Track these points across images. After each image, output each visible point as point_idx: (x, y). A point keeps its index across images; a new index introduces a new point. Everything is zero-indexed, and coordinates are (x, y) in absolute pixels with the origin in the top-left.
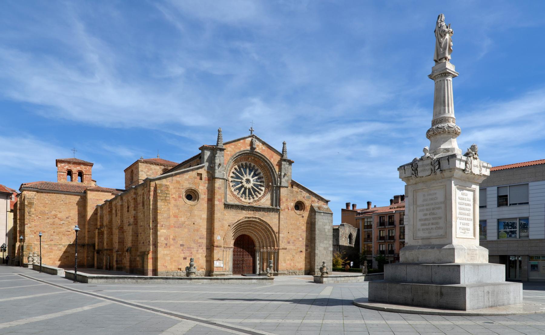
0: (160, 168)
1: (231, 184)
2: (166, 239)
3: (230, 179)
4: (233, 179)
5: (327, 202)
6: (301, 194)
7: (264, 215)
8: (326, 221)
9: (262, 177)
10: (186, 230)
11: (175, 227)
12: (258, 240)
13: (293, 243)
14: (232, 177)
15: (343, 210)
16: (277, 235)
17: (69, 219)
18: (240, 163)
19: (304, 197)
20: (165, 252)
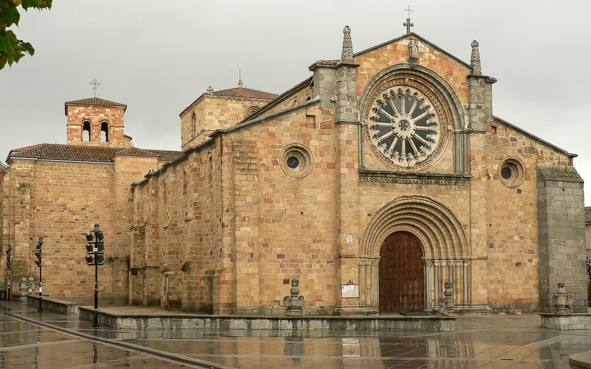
0: (244, 106)
1: (373, 133)
2: (251, 245)
3: (371, 123)
4: (375, 123)
6: (514, 145)
7: (439, 192)
11: (267, 221)
13: (501, 246)
14: (373, 118)
16: (467, 231)
17: (87, 212)
18: (388, 91)
19: (520, 151)
20: (250, 270)
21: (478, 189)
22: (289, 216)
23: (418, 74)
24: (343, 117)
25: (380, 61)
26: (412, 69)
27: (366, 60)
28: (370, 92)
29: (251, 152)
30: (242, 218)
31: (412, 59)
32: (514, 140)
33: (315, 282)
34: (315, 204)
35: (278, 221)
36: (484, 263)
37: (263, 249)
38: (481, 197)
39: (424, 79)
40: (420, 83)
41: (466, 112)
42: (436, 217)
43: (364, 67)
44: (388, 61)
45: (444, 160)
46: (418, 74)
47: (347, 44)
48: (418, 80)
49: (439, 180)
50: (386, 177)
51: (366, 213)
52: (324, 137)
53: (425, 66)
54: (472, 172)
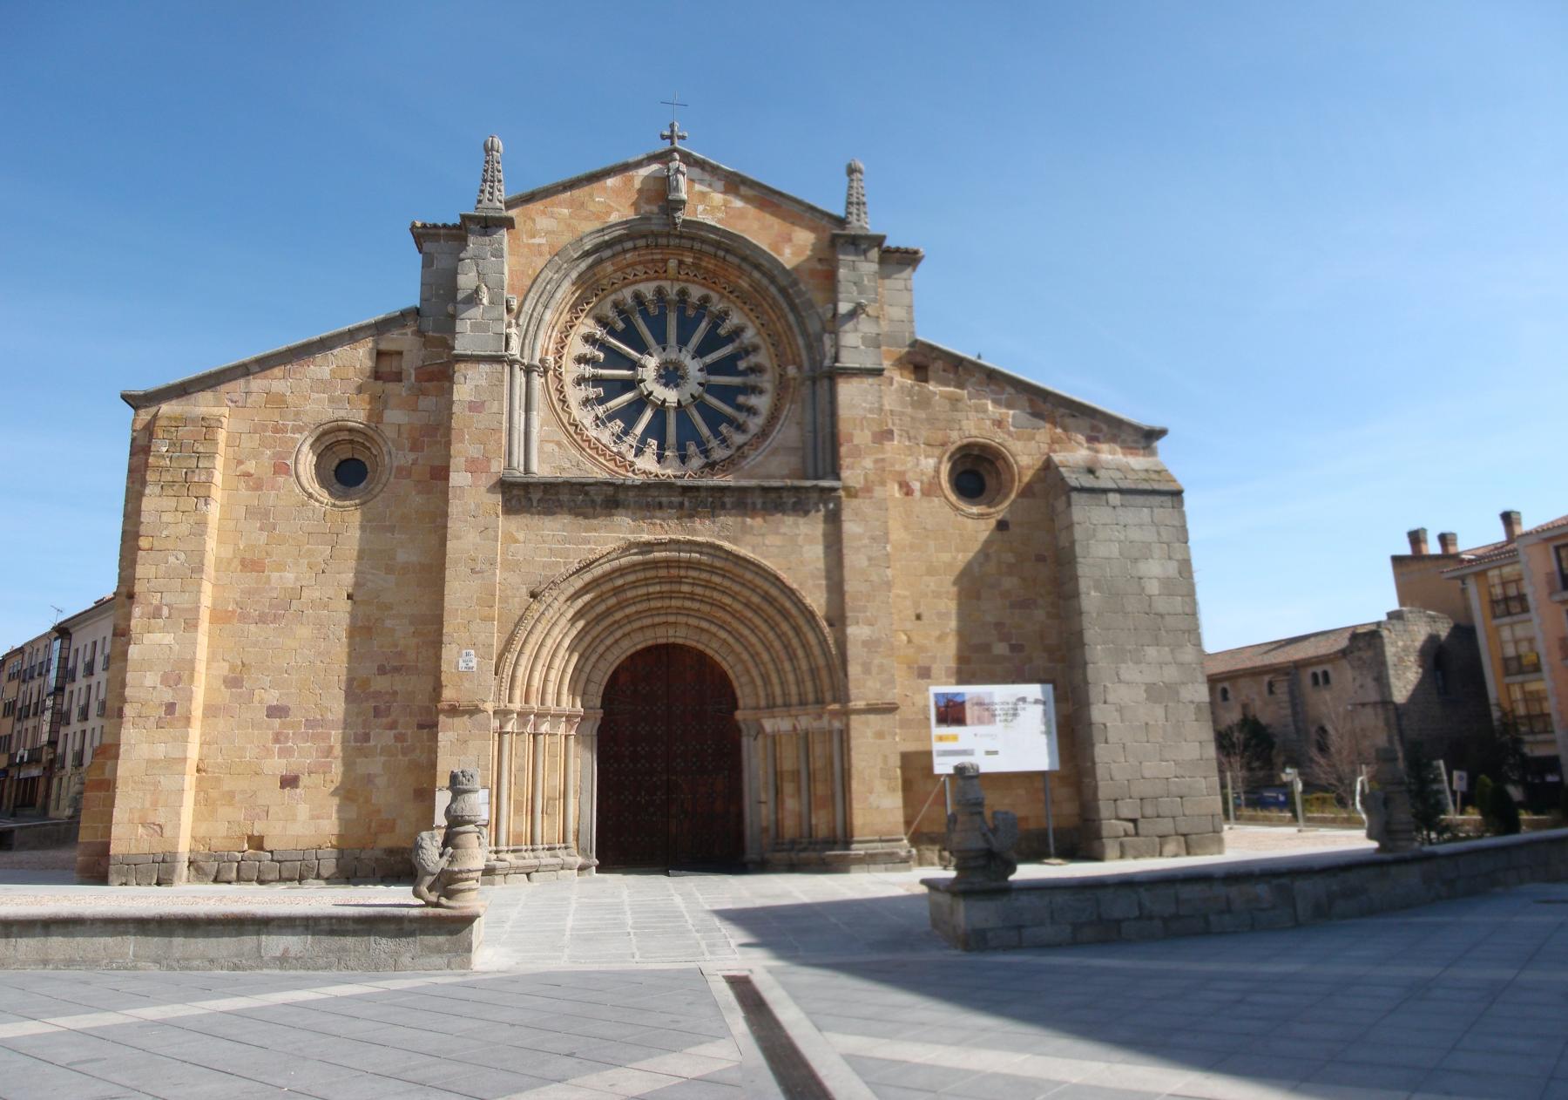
4: (589, 371)
5: (1149, 437)
7: (745, 530)
8: (1149, 535)
9: (756, 349)
10: (304, 632)
11: (243, 618)
15: (1397, 561)
18: (627, 294)
19: (999, 423)
23: (697, 246)
24: (461, 346)
25: (585, 213)
27: (543, 213)
30: (151, 609)
33: (378, 781)
34: (389, 570)
35: (276, 618)
38: (873, 539)
44: (608, 214)
45: (774, 452)
46: (697, 246)
47: (488, 178)
50: (587, 494)
51: (524, 591)
52: (426, 403)
54: (845, 474)
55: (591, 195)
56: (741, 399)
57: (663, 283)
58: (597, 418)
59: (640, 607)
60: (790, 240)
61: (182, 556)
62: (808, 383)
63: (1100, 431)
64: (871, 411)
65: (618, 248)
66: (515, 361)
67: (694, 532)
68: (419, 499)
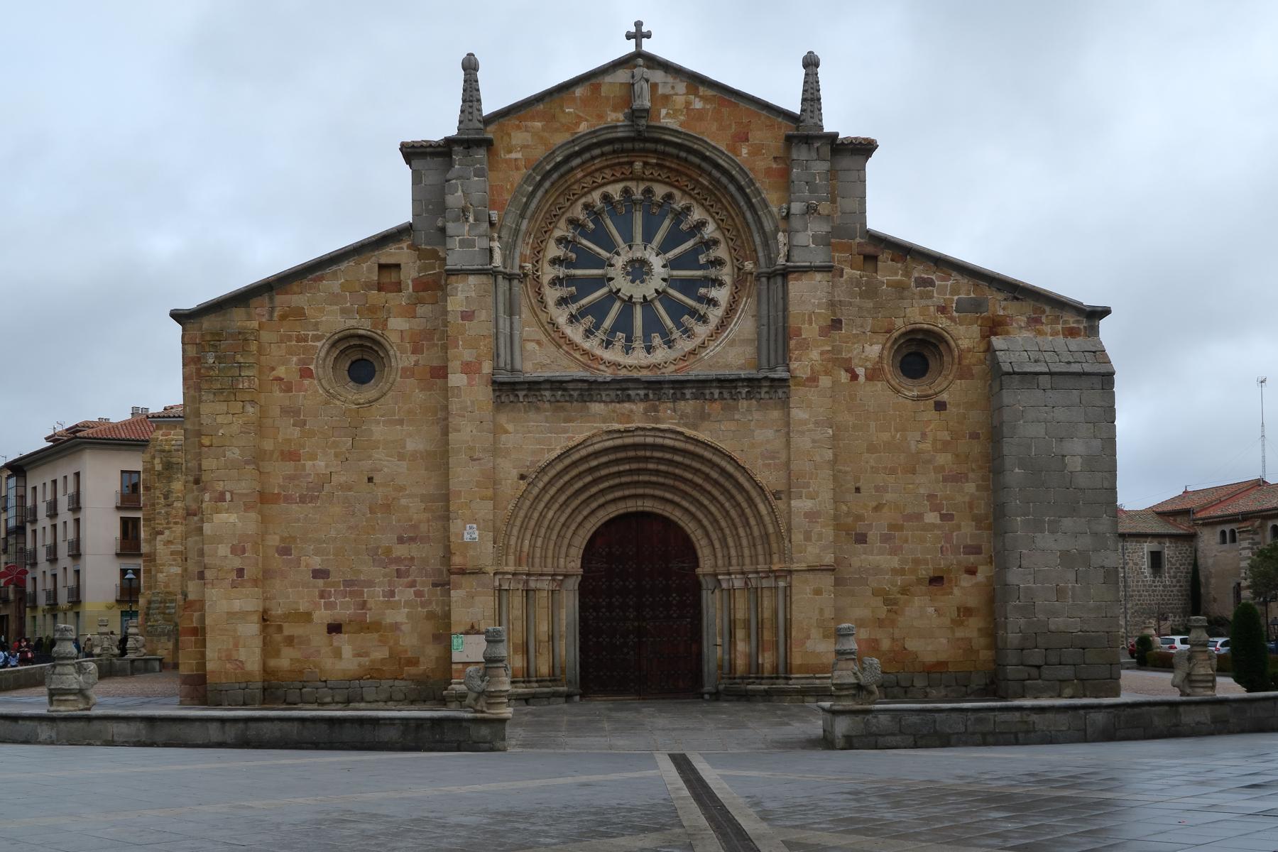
2: (238, 550)
3: (548, 272)
4: (561, 272)
7: (703, 416)
9: (715, 242)
11: (288, 499)
12: (707, 535)
13: (886, 539)
16: (781, 505)
18: (596, 196)
19: (942, 309)
21: (807, 409)
22: (342, 487)
23: (661, 147)
24: (453, 262)
26: (639, 137)
27: (519, 127)
28: (535, 201)
29: (245, 351)
30: (217, 494)
31: (635, 115)
32: (923, 282)
34: (401, 457)
35: (313, 499)
36: (827, 581)
37: (277, 561)
38: (816, 423)
39: (678, 157)
40: (677, 171)
41: (782, 225)
42: (707, 477)
43: (514, 142)
44: (578, 124)
45: (732, 343)
46: (661, 147)
48: (668, 164)
49: (705, 388)
50: (565, 390)
51: (515, 473)
53: (676, 127)
55: (562, 108)
56: (702, 291)
57: (629, 184)
58: (572, 315)
59: (612, 482)
60: (747, 140)
61: (237, 451)
62: (764, 280)
63: (1044, 312)
64: (819, 305)
65: (587, 156)
66: (500, 272)
67: (657, 420)
68: (420, 396)
